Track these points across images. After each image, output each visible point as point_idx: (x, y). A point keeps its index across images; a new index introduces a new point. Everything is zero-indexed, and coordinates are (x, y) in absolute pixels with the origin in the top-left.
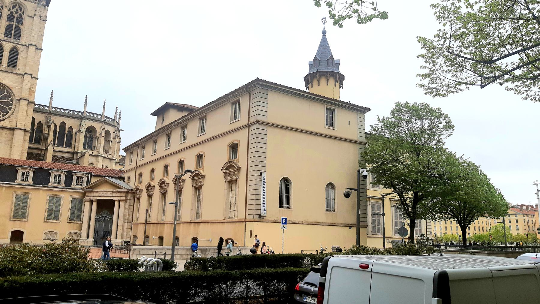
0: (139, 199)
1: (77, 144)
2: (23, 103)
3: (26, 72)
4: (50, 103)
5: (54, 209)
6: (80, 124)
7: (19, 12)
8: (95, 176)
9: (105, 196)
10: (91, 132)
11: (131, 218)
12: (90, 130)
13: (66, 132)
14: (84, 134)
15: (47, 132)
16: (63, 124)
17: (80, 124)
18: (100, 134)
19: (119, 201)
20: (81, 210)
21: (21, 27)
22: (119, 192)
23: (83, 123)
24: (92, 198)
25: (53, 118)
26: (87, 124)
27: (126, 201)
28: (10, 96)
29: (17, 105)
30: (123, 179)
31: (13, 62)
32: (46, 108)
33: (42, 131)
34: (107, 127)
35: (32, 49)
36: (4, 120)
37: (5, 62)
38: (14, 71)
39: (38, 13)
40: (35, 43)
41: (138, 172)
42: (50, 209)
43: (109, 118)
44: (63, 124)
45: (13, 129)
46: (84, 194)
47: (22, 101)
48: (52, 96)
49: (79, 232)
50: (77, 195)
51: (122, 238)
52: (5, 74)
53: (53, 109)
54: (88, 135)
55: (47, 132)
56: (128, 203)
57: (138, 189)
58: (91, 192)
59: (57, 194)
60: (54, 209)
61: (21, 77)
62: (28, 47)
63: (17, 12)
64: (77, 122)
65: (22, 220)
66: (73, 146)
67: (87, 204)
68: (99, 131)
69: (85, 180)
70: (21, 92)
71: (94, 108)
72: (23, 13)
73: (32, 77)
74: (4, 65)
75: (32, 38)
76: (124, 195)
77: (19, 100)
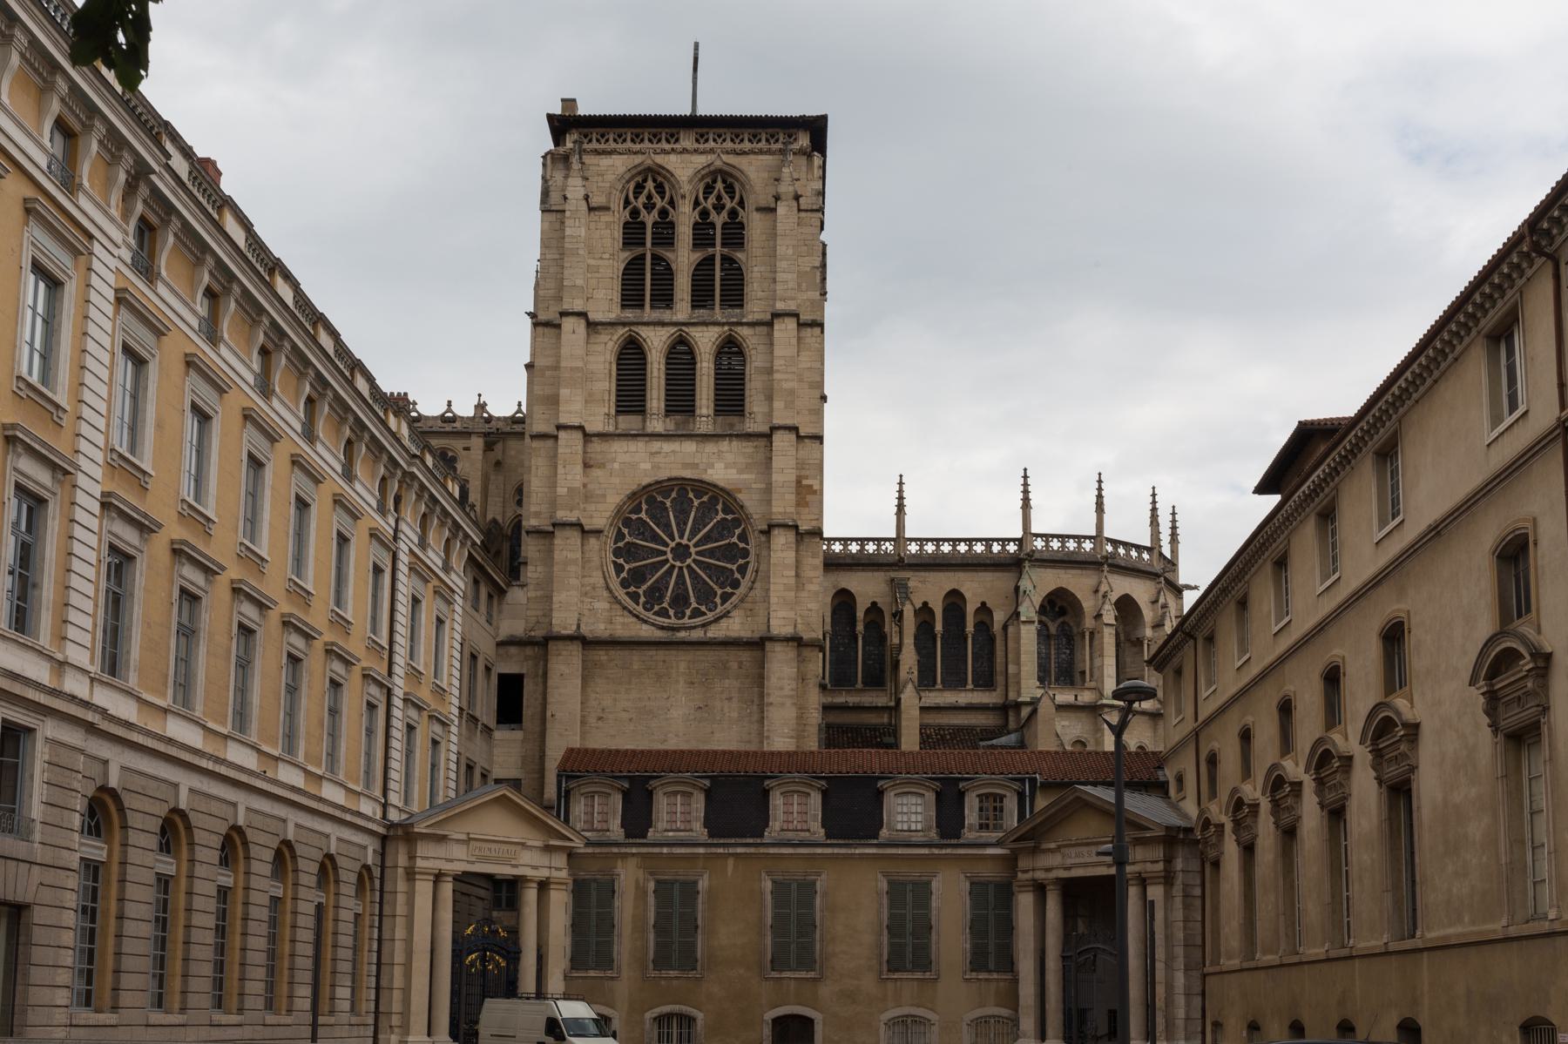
0: (1216, 864)
1: (1012, 669)
2: (781, 539)
3: (777, 421)
5: (909, 927)
7: (729, 205)
8: (1047, 786)
9: (1085, 865)
12: (1059, 606)
13: (970, 628)
16: (955, 600)
17: (1017, 588)
18: (1098, 616)
20: (1007, 927)
21: (740, 255)
23: (1025, 584)
24: (1040, 875)
25: (915, 580)
26: (1039, 584)
27: (1168, 879)
28: (737, 522)
29: (764, 553)
30: (1160, 788)
31: (731, 399)
32: (889, 547)
34: (1121, 585)
35: (785, 331)
36: (726, 615)
37: (704, 402)
38: (738, 429)
39: (785, 188)
40: (791, 306)
42: (895, 927)
43: (1126, 545)
44: (955, 600)
45: (759, 644)
46: (1011, 861)
47: (776, 532)
48: (901, 498)
50: (989, 872)
52: (710, 447)
54: (1053, 629)
55: (896, 640)
58: (1035, 851)
59: (913, 872)
60: (909, 927)
61: (762, 442)
62: (770, 324)
63: (719, 207)
66: (1000, 679)
68: (1088, 604)
69: (1011, 804)
70: (769, 502)
71: (1062, 514)
72: (741, 203)
73: (799, 437)
74: (704, 411)
75: (779, 287)
77: (767, 532)
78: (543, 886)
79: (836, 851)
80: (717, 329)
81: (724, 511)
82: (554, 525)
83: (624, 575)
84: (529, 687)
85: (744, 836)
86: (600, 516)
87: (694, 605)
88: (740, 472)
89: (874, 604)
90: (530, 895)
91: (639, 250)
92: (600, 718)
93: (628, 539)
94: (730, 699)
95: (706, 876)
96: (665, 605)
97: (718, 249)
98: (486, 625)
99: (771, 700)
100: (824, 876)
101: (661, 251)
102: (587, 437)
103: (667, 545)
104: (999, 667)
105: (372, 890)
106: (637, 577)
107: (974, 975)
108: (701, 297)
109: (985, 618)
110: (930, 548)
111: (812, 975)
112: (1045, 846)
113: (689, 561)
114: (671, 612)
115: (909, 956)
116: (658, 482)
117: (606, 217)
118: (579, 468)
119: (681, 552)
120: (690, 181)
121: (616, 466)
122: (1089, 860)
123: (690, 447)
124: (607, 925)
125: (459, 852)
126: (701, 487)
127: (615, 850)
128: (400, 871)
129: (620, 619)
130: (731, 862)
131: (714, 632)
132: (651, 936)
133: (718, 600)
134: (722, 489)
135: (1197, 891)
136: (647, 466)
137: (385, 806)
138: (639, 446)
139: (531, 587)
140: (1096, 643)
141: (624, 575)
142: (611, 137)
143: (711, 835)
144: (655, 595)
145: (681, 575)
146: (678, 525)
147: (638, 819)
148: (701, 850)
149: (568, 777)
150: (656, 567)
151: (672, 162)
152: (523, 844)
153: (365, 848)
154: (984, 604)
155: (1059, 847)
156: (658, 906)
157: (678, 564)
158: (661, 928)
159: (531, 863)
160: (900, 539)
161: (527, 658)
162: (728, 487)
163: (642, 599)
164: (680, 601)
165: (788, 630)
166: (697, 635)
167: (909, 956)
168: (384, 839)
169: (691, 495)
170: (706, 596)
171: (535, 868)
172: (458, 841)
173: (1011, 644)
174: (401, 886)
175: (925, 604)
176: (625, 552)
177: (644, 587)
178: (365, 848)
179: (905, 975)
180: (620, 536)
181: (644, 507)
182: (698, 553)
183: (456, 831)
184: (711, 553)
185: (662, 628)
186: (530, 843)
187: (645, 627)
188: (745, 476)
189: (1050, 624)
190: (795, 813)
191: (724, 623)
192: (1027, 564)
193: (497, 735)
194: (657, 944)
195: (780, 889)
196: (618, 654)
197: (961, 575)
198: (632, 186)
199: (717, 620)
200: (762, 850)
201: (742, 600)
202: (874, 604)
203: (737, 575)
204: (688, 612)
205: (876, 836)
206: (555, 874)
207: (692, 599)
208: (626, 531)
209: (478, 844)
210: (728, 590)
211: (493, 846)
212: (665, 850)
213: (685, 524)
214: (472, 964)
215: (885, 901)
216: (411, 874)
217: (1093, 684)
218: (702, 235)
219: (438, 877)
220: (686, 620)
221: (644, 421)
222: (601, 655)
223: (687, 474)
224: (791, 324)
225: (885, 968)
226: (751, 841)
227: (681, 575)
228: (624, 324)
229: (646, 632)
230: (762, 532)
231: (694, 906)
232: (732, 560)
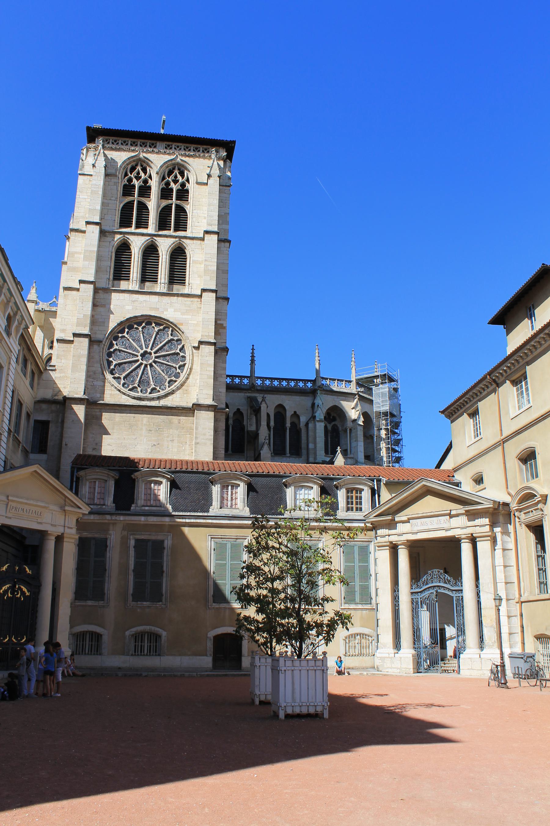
1: (311, 446)
4: (252, 371)
6: (313, 405)
10: (334, 419)
13: (288, 425)
14: (323, 424)
15: (253, 428)
16: (280, 411)
17: (313, 405)
23: (318, 401)
32: (246, 381)
33: (243, 428)
36: (173, 392)
44: (280, 411)
48: (253, 356)
54: (329, 427)
64: (306, 401)
66: (304, 452)
67: (385, 555)
69: (366, 495)
72: (188, 180)
80: (173, 240)
84: (52, 429)
88: (183, 314)
89: (238, 409)
90: (51, 545)
91: (130, 199)
92: (94, 449)
94: (172, 441)
97: (174, 201)
101: (143, 199)
103: (138, 352)
104: (304, 445)
109: (295, 420)
116: (136, 317)
117: (114, 180)
118: (90, 304)
120: (161, 167)
123: (154, 299)
124: (101, 569)
126: (159, 321)
131: (162, 403)
132: (131, 578)
133: (167, 384)
134: (171, 323)
136: (130, 308)
140: (353, 434)
142: (120, 142)
149: (79, 469)
151: (151, 157)
154: (295, 412)
156: (137, 557)
157: (145, 362)
158: (139, 571)
160: (251, 377)
170: (159, 381)
173: (311, 433)
185: (134, 398)
188: (184, 317)
191: (170, 397)
194: (135, 583)
197: (283, 397)
198: (130, 167)
199: (166, 395)
202: (238, 409)
207: (152, 383)
213: (150, 340)
217: (352, 456)
218: (165, 193)
221: (129, 284)
223: (153, 313)
224: (215, 237)
226: (201, 514)
228: (121, 233)
230: (194, 347)
231: (161, 557)
232: (176, 362)
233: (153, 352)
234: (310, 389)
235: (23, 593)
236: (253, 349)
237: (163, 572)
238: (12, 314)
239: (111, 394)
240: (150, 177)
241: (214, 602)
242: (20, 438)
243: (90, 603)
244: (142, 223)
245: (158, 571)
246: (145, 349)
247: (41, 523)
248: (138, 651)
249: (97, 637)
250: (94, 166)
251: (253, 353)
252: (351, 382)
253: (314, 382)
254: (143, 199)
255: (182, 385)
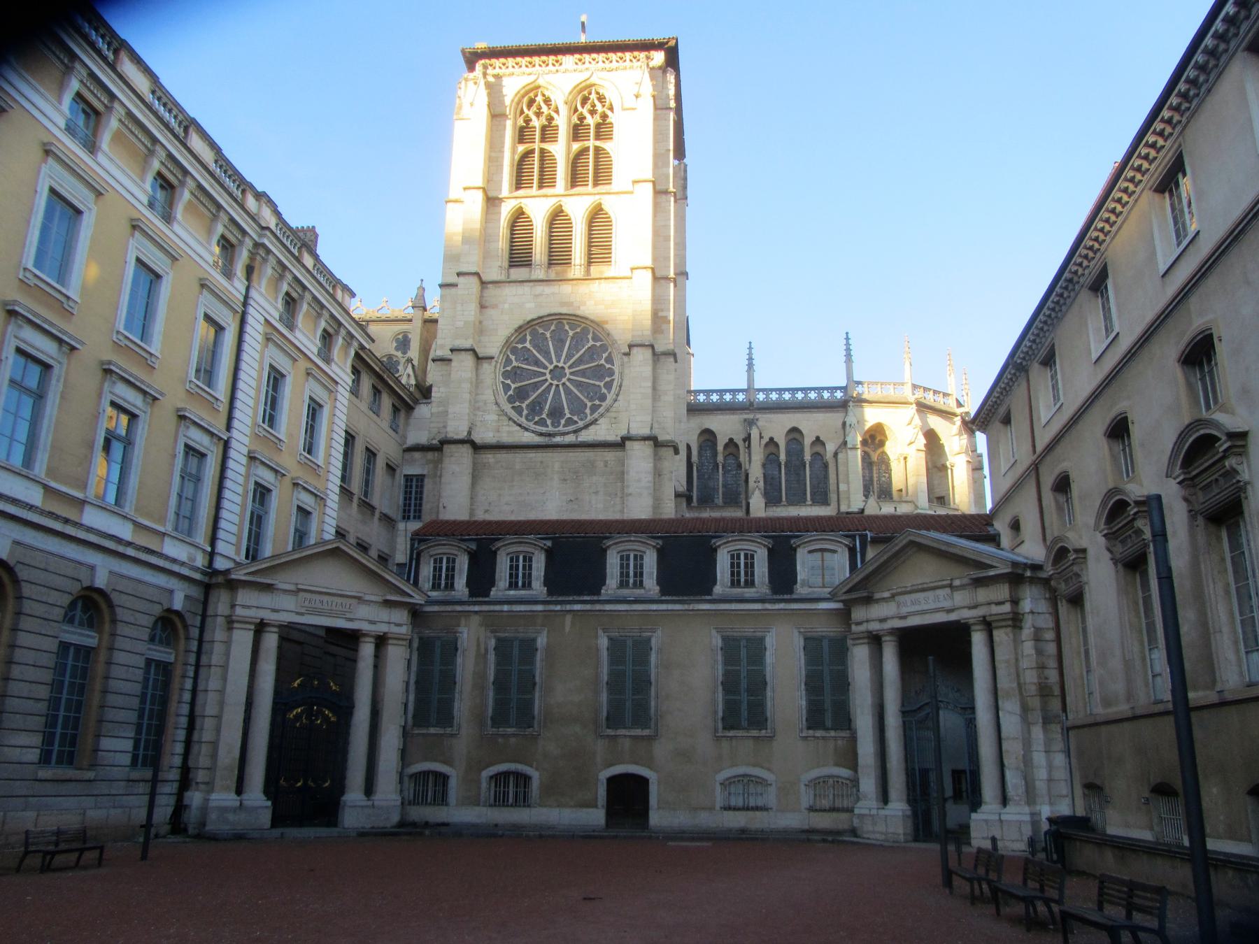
0: (1077, 600)
1: (842, 487)
4: (750, 380)
5: (744, 685)
6: (844, 424)
8: (875, 541)
11: (1055, 705)
17: (844, 424)
19: (988, 625)
20: (842, 683)
22: (979, 582)
24: (874, 626)
32: (741, 397)
36: (594, 422)
41: (1048, 480)
42: (730, 684)
45: (621, 444)
46: (845, 615)
48: (750, 359)
49: (845, 772)
51: (1030, 796)
53: (761, 397)
56: (1027, 632)
57: (1061, 554)
58: (869, 600)
59: (748, 629)
60: (744, 685)
64: (834, 419)
65: (638, 732)
66: (833, 497)
72: (611, 109)
76: (1003, 591)
78: (381, 641)
79: (670, 607)
81: (594, 339)
82: (452, 350)
83: (511, 392)
85: (581, 594)
86: (493, 345)
87: (568, 415)
89: (731, 440)
90: (367, 650)
92: (486, 511)
93: (515, 364)
95: (545, 633)
96: (544, 416)
97: (592, 143)
98: (390, 431)
99: (631, 490)
100: (659, 632)
101: (546, 146)
102: (483, 283)
103: (546, 368)
104: (832, 487)
105: (188, 638)
106: (521, 394)
107: (811, 732)
108: (575, 179)
109: (818, 449)
110: (774, 396)
111: (646, 732)
112: (877, 596)
113: (564, 380)
114: (549, 422)
115: (745, 714)
119: (557, 372)
121: (506, 306)
122: (926, 607)
124: (449, 682)
125: (288, 602)
127: (459, 608)
128: (220, 620)
129: (506, 429)
130: (568, 618)
131: (585, 436)
132: (491, 694)
133: (588, 411)
135: (1050, 635)
137: (212, 555)
138: (526, 288)
139: (434, 404)
141: (511, 392)
143: (550, 593)
144: (535, 408)
145: (557, 392)
146: (556, 352)
147: (481, 581)
148: (540, 608)
149: (420, 541)
150: (536, 386)
152: (359, 598)
153: (171, 592)
154: (818, 438)
155: (893, 596)
156: (498, 664)
157: (555, 382)
158: (501, 685)
159: (369, 616)
161: (429, 462)
162: (597, 319)
163: (525, 412)
164: (556, 413)
165: (646, 431)
166: (570, 439)
167: (745, 714)
168: (207, 588)
169: (567, 327)
170: (579, 409)
171: (372, 622)
172: (285, 591)
174: (219, 635)
175: (771, 439)
176: (514, 374)
177: (527, 402)
178: (171, 592)
179: (740, 733)
180: (508, 361)
181: (529, 338)
182: (571, 374)
183: (283, 581)
184: (583, 373)
185: (541, 434)
186: (367, 598)
187: (527, 434)
189: (872, 453)
190: (633, 573)
191: (592, 428)
192: (851, 404)
193: (401, 526)
195: (616, 647)
196: (503, 456)
198: (526, 100)
199: (586, 427)
200: (598, 607)
201: (608, 410)
202: (731, 440)
203: (604, 390)
204: (563, 422)
205: (710, 592)
206: (395, 629)
207: (567, 411)
208: (513, 358)
209: (308, 596)
210: (597, 402)
211: (326, 598)
212: (506, 608)
214: (298, 717)
215: (720, 658)
216: (230, 623)
219: (261, 628)
220: (561, 428)
222: (489, 457)
223: (564, 310)
225: (720, 725)
226: (587, 598)
227: (557, 392)
229: (528, 438)
231: (532, 663)
232: (601, 378)
233: (566, 366)
234: (839, 401)
235: (326, 718)
236: (750, 348)
237: (535, 684)
238: (331, 330)
239: (509, 432)
240: (557, 111)
241: (608, 727)
242: (375, 501)
243: (432, 730)
244: (546, 180)
245: (528, 684)
246: (555, 363)
247: (351, 620)
248: (500, 800)
249: (442, 779)
250: (472, 104)
251: (750, 354)
252: (903, 384)
253: (844, 389)
254: (546, 146)
255: (608, 410)
